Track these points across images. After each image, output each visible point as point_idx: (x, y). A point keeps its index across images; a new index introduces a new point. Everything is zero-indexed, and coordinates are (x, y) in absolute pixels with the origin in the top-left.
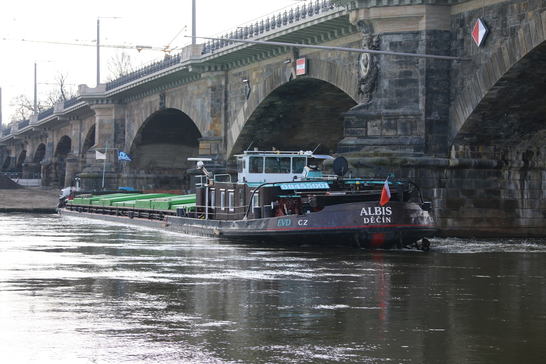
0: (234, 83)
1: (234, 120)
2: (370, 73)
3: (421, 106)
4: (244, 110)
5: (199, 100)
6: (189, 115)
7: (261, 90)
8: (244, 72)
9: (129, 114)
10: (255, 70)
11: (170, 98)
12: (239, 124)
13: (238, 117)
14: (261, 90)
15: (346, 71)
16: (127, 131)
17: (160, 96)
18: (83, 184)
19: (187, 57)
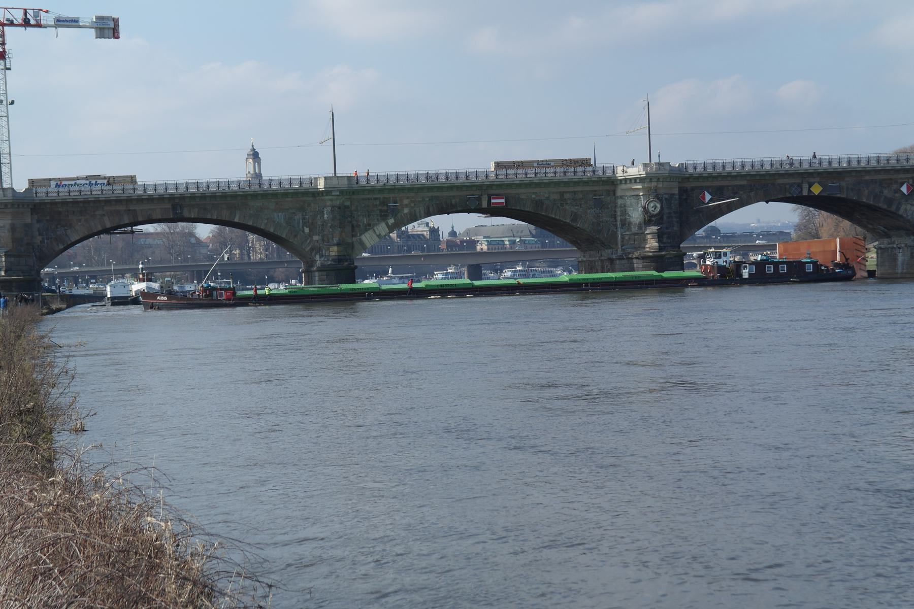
0: (363, 205)
1: (366, 230)
2: (660, 212)
3: (675, 228)
4: (387, 224)
5: (280, 214)
6: (255, 225)
7: (420, 212)
8: (384, 198)
9: (48, 218)
10: (408, 198)
11: (196, 210)
12: (378, 233)
13: (375, 228)
14: (420, 212)
15: (558, 207)
16: (40, 235)
17: (172, 206)
18: (13, 289)
19: (338, 184)
